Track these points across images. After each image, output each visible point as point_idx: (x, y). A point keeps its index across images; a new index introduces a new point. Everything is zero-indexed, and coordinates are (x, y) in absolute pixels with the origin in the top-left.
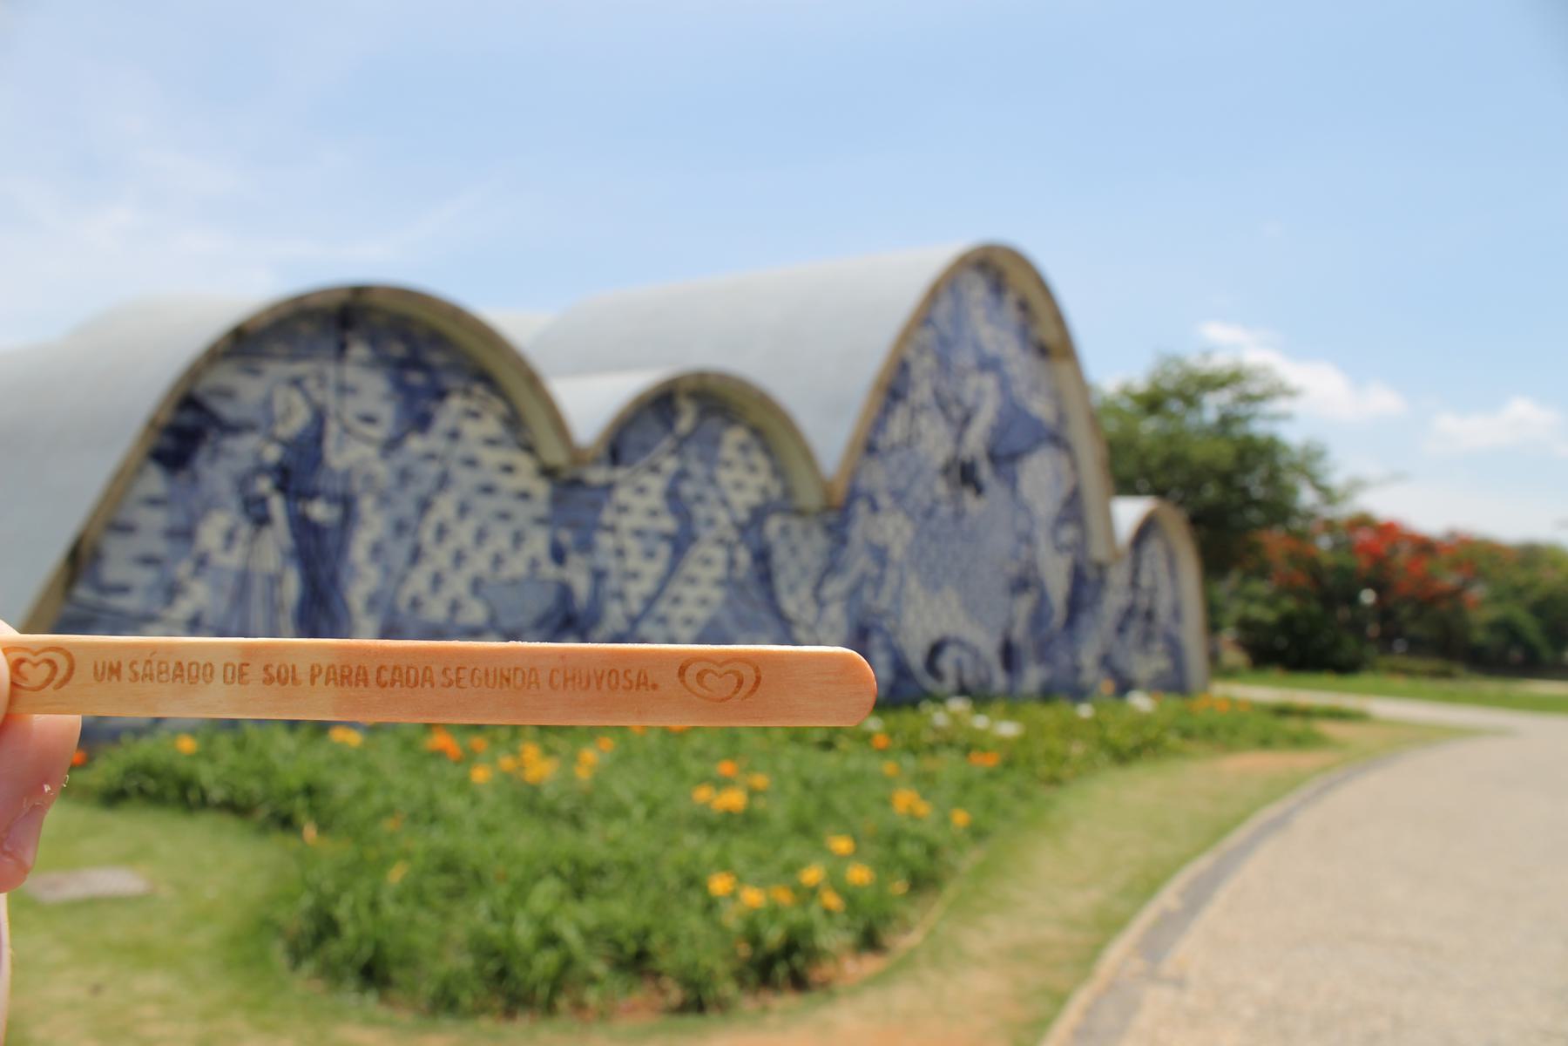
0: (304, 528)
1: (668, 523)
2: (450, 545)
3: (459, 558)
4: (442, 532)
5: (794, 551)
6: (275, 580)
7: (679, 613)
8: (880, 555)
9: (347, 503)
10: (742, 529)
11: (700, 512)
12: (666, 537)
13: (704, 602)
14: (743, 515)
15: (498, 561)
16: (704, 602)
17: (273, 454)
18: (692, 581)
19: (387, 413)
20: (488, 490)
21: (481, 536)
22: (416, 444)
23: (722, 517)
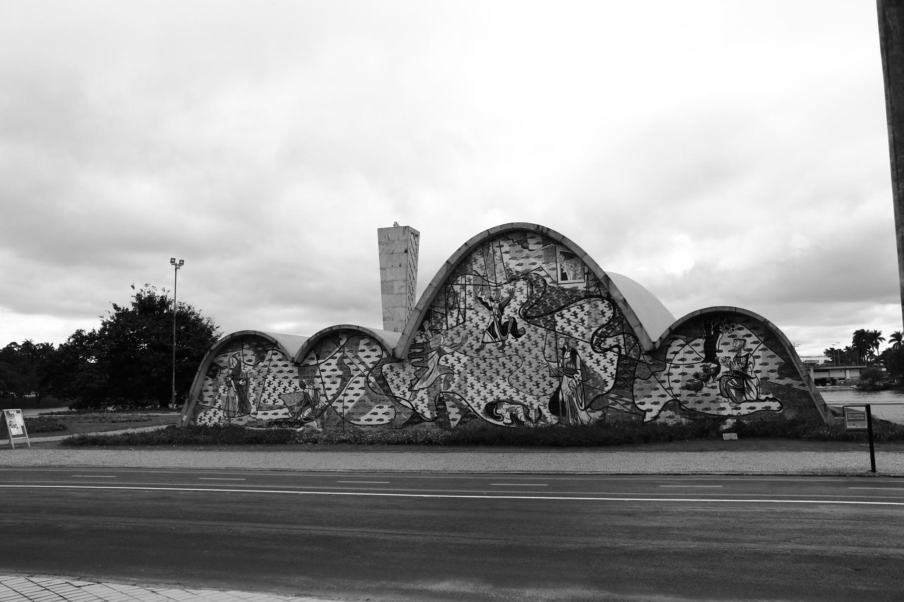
0: (238, 387)
1: (340, 373)
2: (272, 386)
3: (274, 389)
4: (269, 383)
5: (398, 374)
6: (233, 398)
7: (347, 399)
8: (450, 371)
9: (247, 380)
10: (370, 370)
11: (352, 367)
12: (338, 376)
13: (357, 395)
14: (371, 366)
15: (285, 389)
16: (357, 395)
17: (231, 372)
18: (352, 389)
19: (254, 358)
20: (281, 372)
21: (279, 383)
22: (261, 364)
23: (362, 367)
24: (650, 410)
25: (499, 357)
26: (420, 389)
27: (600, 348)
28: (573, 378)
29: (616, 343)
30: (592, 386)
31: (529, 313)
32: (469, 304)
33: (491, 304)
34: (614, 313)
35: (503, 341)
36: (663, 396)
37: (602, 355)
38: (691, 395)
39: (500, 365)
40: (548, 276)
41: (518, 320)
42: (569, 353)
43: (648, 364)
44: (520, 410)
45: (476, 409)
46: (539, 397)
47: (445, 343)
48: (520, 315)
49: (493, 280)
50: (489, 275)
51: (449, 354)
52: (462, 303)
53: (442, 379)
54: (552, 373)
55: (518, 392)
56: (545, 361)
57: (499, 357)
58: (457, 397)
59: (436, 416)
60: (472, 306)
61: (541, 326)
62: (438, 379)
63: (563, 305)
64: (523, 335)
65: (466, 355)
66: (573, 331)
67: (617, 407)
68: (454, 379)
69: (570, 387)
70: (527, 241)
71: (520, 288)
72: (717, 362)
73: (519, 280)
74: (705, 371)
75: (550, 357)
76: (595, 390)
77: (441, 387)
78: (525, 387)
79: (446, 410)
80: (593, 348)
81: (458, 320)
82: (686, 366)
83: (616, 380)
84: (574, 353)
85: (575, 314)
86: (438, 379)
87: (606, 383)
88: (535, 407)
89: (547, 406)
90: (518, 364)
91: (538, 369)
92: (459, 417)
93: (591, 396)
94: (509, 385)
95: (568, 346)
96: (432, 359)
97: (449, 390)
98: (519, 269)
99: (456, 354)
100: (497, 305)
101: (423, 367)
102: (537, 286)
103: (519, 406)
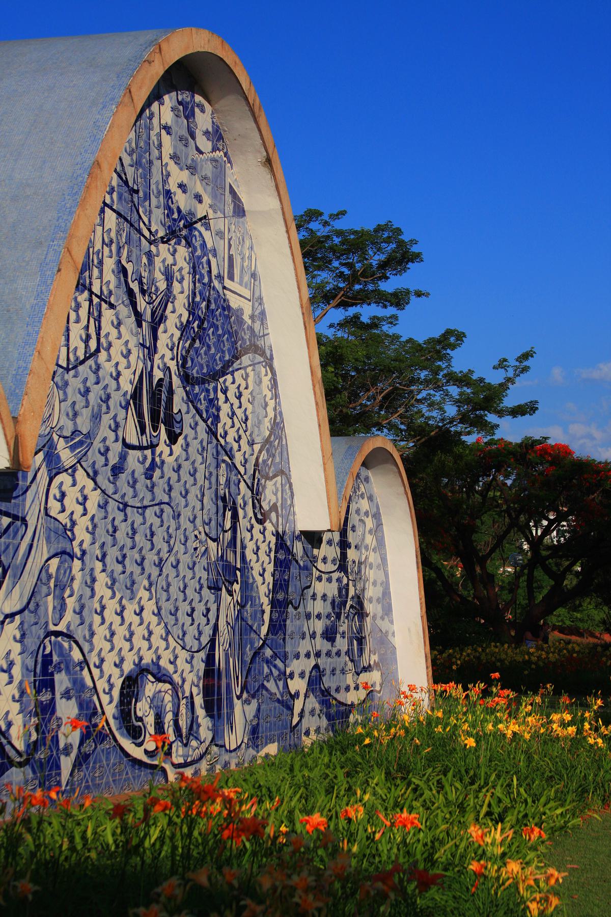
24: (297, 694)
25: (146, 507)
26: (7, 616)
27: (261, 507)
28: (230, 593)
29: (274, 500)
30: (250, 623)
31: (189, 364)
32: (108, 283)
33: (142, 304)
34: (275, 409)
35: (153, 446)
36: (308, 655)
37: (261, 527)
38: (328, 654)
39: (146, 536)
40: (215, 252)
41: (176, 381)
42: (230, 513)
43: (300, 566)
44: (168, 698)
45: (105, 699)
46: (192, 657)
47: (61, 423)
48: (178, 369)
49: (145, 214)
50: (141, 194)
51: (66, 470)
52: (96, 272)
53: (49, 577)
54: (211, 576)
55: (168, 633)
56: (203, 536)
57: (146, 507)
58: (76, 655)
59: (34, 736)
60: (110, 293)
61: (201, 417)
62: (44, 574)
63: (227, 358)
64: (180, 434)
65: (97, 486)
66: (235, 446)
67: (271, 685)
68: (73, 579)
69: (228, 623)
70: (193, 114)
71: (180, 270)
72: (346, 573)
73: (179, 243)
74: (340, 590)
75: (210, 520)
76: (253, 635)
77: (47, 610)
78: (177, 620)
79: (53, 711)
80: (254, 507)
81: (88, 337)
82: (327, 576)
83: (274, 603)
84: (235, 517)
85: (239, 397)
86: (44, 574)
87: (263, 612)
88: (187, 687)
89: (201, 685)
90: (170, 537)
91: (194, 559)
92: (75, 737)
93: (249, 654)
94: (156, 611)
95: (229, 492)
96: (34, 486)
97: (61, 627)
98: (182, 200)
99: (80, 474)
100: (149, 312)
101: (15, 518)
102: (202, 276)
103: (168, 686)
